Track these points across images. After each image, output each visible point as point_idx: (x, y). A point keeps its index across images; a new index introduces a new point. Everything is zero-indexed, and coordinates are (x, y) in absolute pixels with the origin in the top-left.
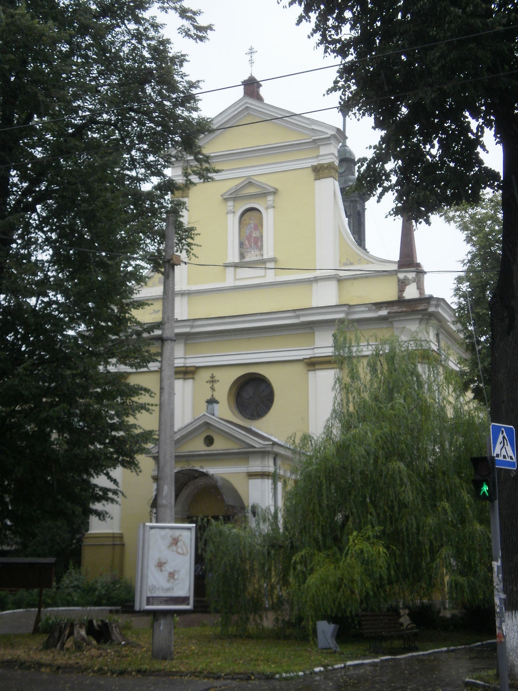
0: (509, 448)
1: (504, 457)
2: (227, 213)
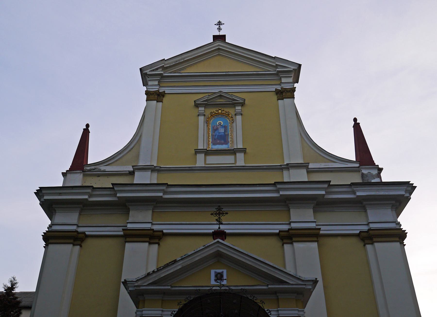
2: (198, 115)
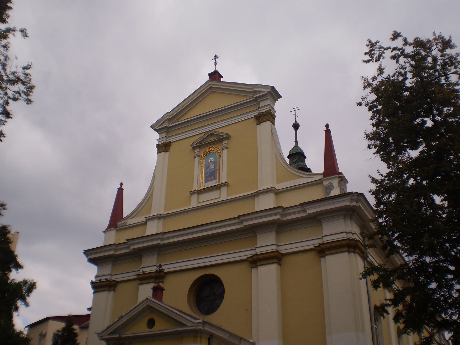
2: (195, 157)
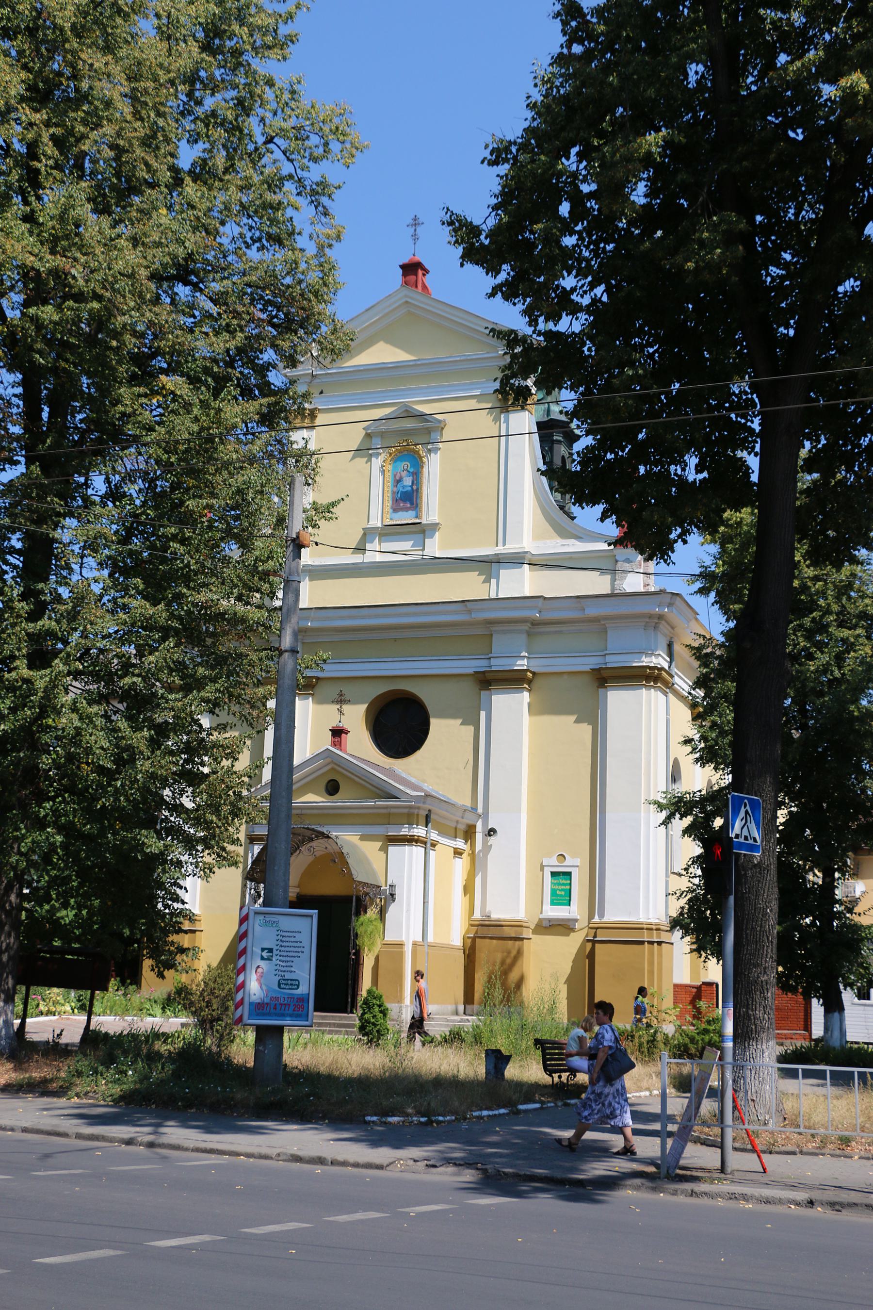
0: (753, 826)
1: (746, 838)
